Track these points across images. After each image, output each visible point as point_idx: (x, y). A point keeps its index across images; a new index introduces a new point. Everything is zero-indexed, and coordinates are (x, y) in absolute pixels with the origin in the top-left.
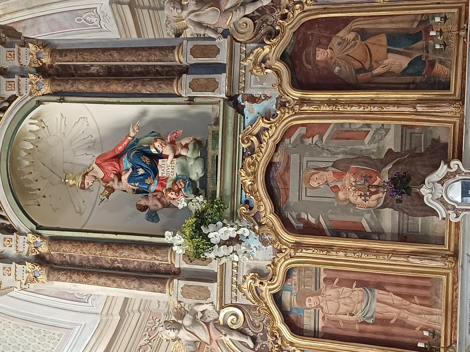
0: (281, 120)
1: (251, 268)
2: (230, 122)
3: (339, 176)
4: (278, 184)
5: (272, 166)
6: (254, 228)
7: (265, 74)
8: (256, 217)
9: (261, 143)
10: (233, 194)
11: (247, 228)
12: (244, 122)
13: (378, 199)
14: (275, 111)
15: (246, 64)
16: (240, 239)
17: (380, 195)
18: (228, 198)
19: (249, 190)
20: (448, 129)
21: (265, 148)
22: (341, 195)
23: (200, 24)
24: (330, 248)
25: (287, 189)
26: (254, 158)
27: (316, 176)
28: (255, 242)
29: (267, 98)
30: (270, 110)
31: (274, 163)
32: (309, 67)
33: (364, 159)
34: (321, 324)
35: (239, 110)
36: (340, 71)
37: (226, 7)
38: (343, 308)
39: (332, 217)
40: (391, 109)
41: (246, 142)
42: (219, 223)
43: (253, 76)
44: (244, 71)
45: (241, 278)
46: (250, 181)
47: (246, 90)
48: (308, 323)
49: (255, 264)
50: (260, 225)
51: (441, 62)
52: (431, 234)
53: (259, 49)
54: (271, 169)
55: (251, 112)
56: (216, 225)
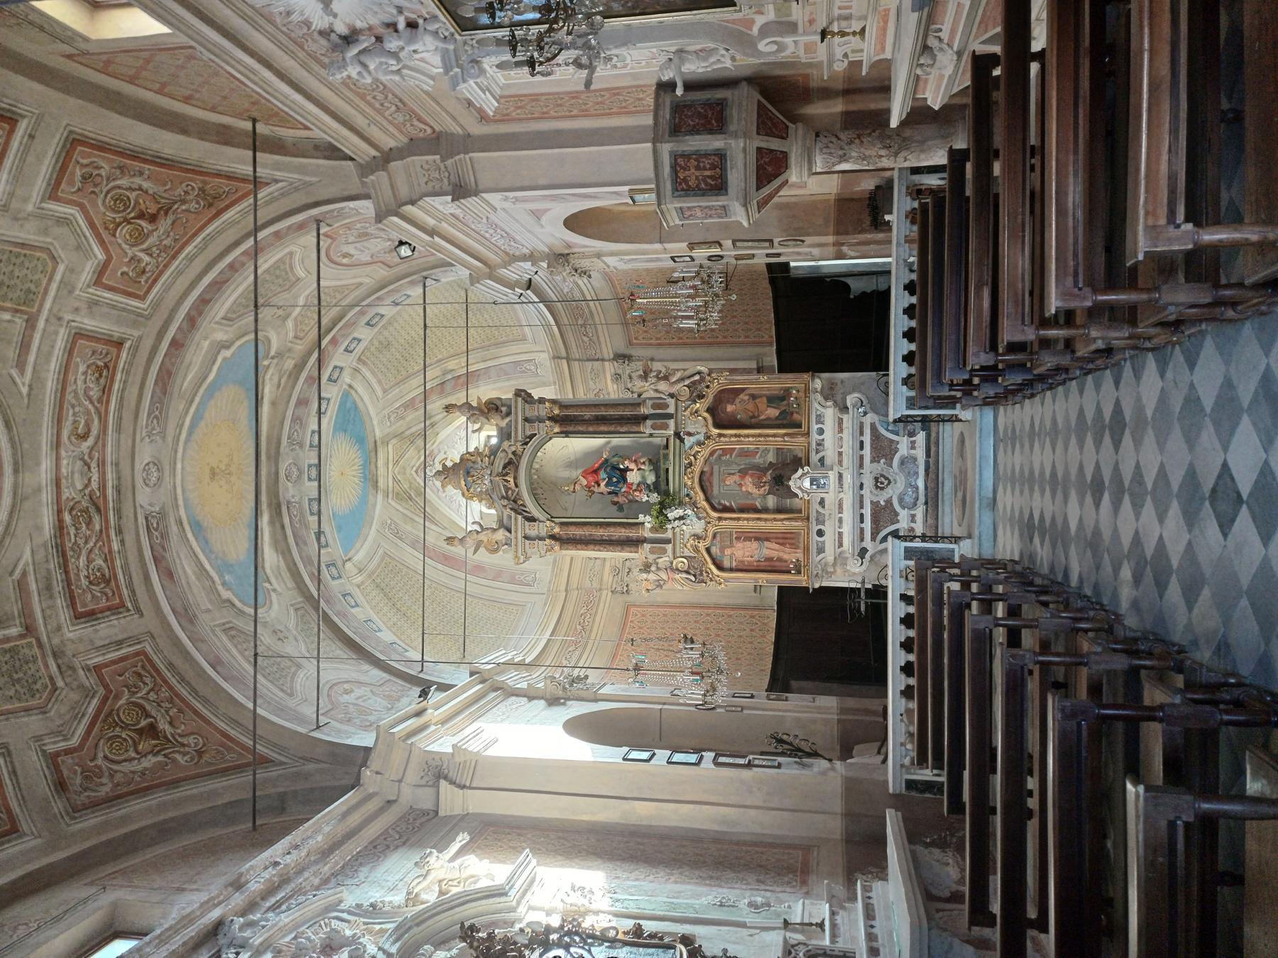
3: (742, 478)
23: (656, 391)
24: (738, 519)
33: (757, 468)
35: (682, 441)
48: (727, 564)
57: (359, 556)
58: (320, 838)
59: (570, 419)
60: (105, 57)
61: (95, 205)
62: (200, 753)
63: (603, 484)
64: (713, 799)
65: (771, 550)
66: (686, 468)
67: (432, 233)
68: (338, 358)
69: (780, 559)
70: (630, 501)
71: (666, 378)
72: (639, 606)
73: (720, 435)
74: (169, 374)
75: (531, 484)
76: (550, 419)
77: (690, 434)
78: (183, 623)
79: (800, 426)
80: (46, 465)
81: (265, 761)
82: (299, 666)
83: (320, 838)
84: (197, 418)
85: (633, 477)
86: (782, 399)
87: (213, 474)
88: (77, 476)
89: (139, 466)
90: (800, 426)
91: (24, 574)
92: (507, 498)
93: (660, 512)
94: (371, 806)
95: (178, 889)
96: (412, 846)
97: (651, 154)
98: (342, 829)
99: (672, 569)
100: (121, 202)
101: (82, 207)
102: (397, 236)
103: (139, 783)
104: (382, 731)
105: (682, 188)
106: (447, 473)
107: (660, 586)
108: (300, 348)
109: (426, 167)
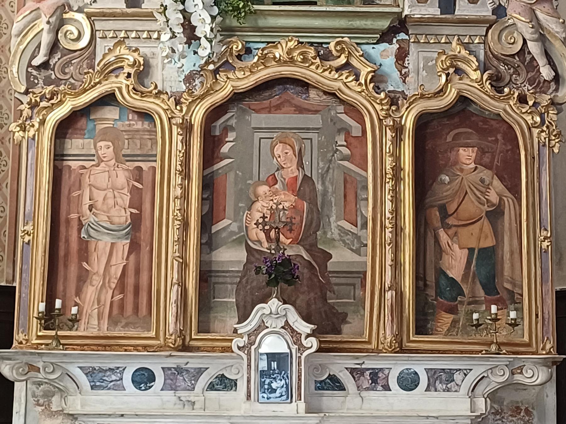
0: (371, 100)
1: (151, 60)
2: (368, 23)
3: (291, 186)
4: (276, 96)
5: (303, 86)
6: (210, 63)
7: (439, 74)
8: (227, 66)
9: (337, 70)
10: (260, 30)
11: (210, 54)
12: (367, 44)
13: (259, 242)
14: (384, 91)
15: (454, 43)
16: (193, 41)
17: (266, 245)
18: (253, 22)
19: (266, 54)
20: (361, 334)
21: (329, 76)
22: (263, 189)
24: (186, 174)
26: (314, 61)
27: (290, 152)
28: (190, 64)
29: (404, 77)
30: (386, 82)
31: (307, 90)
32: (449, 139)
34: (74, 165)
35: (386, 36)
36: (443, 182)
37: (538, 13)
38: (99, 196)
39: (231, 177)
40: (389, 257)
41: (338, 48)
42: (216, 11)
43: (436, 55)
44: (443, 41)
45: (134, 44)
46: (280, 56)
47: (416, 45)
48: (75, 145)
49: (157, 65)
50: (216, 72)
51: (455, 323)
52: (212, 315)
53: (475, 64)
54: (298, 86)
55: (383, 54)
56: (212, 6)
65: (108, 256)
69: (83, 277)
73: (398, 130)
79: (421, 329)
86: (491, 287)
90: (421, 329)
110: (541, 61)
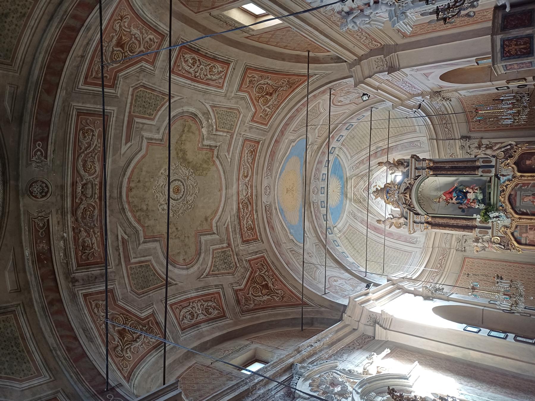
9: (507, 188)
23: (485, 154)
24: (531, 219)
25: (516, 202)
29: (508, 175)
35: (499, 179)
48: (523, 241)
57: (340, 226)
58: (328, 339)
59: (438, 168)
60: (258, 36)
61: (252, 91)
62: (283, 297)
63: (454, 199)
64: (513, 357)
66: (501, 192)
67: (377, 88)
68: (334, 144)
70: (469, 207)
71: (491, 148)
72: (471, 258)
73: (521, 176)
74: (274, 153)
75: (418, 198)
76: (428, 168)
77: (503, 175)
78: (277, 247)
80: (235, 186)
81: (305, 304)
82: (317, 268)
83: (328, 339)
84: (283, 168)
85: (471, 196)
87: (288, 191)
88: (244, 191)
89: (263, 188)
91: (228, 225)
92: (406, 204)
93: (485, 214)
94: (347, 330)
95: (277, 348)
96: (364, 350)
97: (490, 40)
98: (336, 337)
99: (491, 242)
100: (261, 89)
101: (248, 92)
102: (361, 92)
103: (262, 305)
104: (351, 299)
105: (507, 55)
106: (378, 192)
107: (484, 250)
108: (320, 141)
109: (377, 61)
110: (506, 148)
